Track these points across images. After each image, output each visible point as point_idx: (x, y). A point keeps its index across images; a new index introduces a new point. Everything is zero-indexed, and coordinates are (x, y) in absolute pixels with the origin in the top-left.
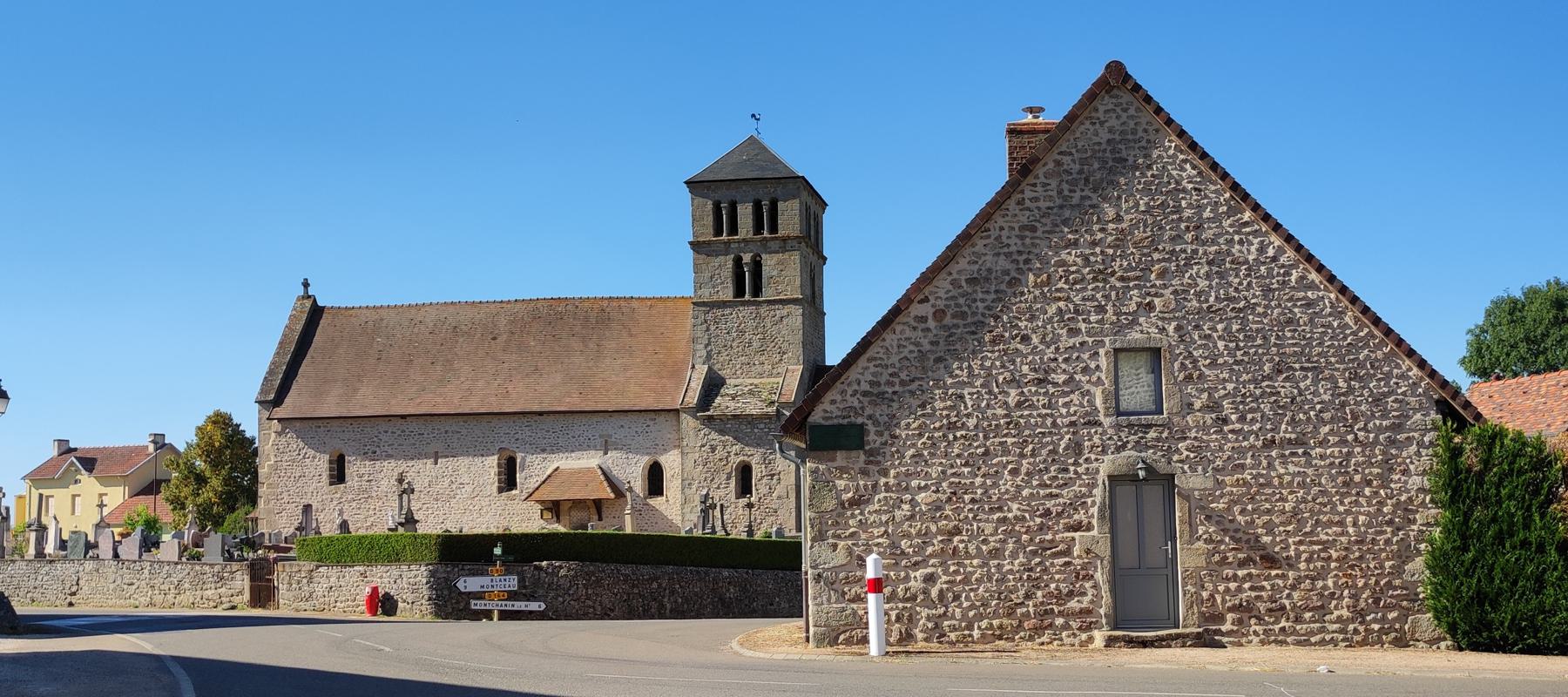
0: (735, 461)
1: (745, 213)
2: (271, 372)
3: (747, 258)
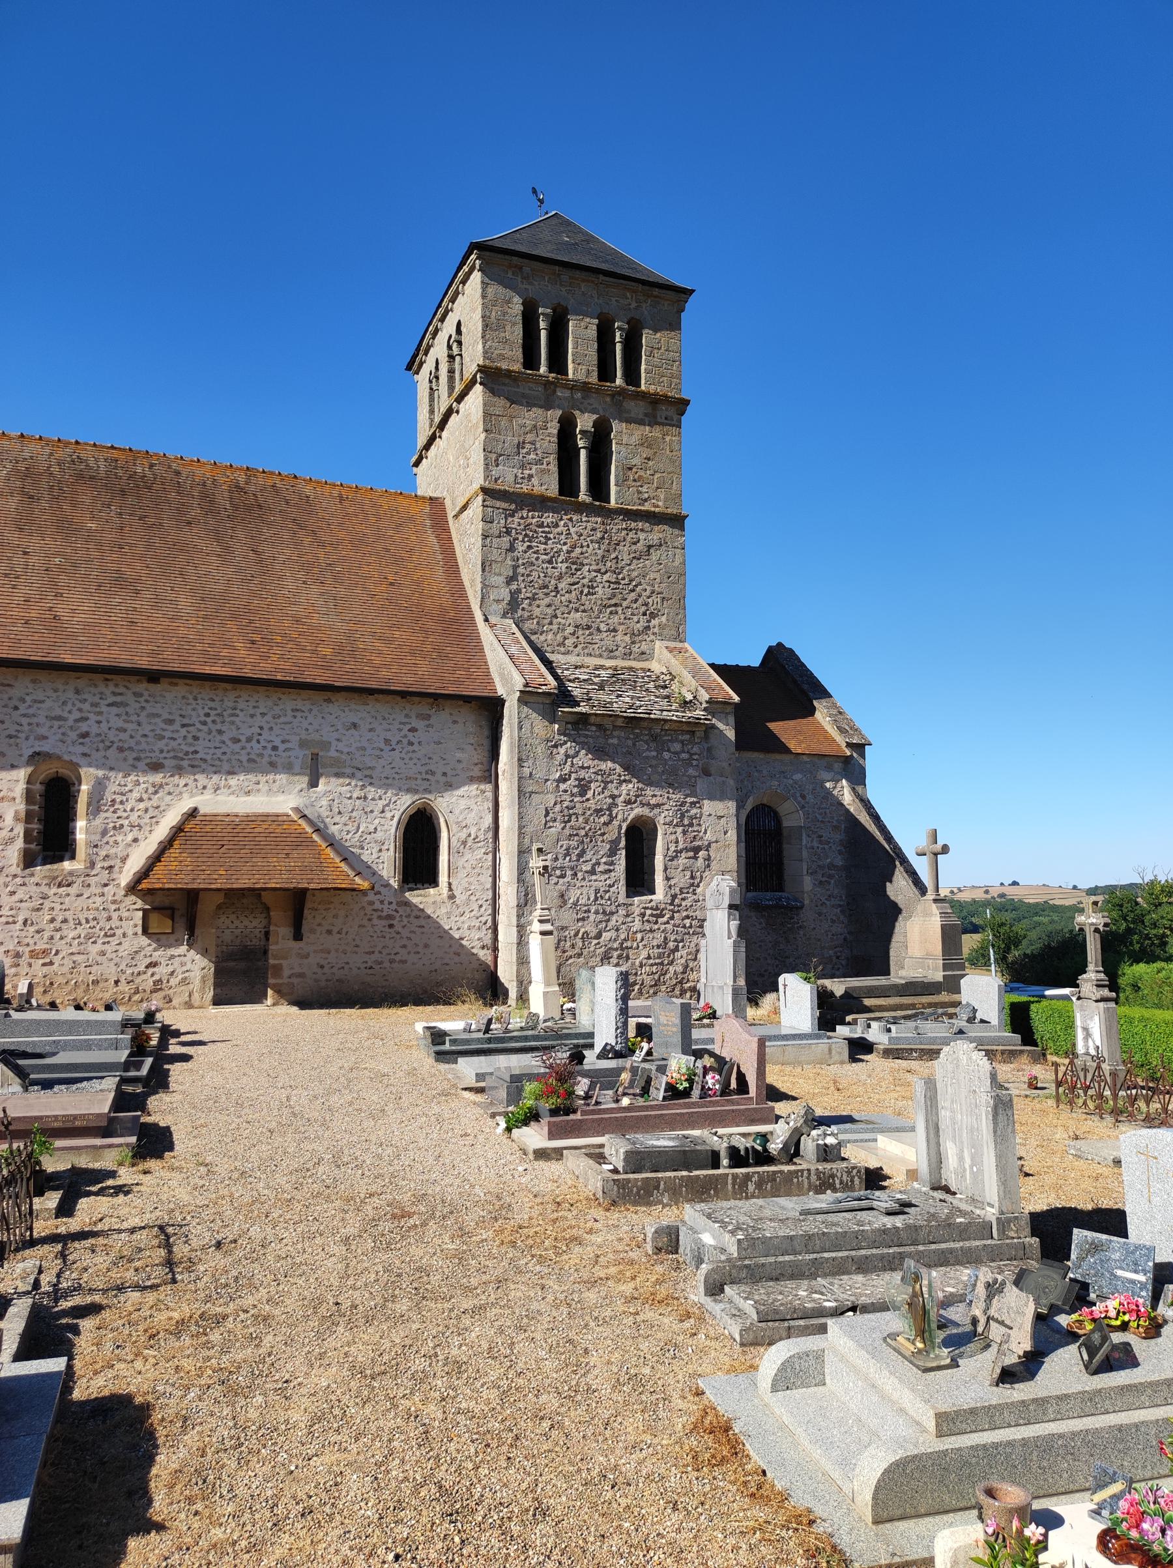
0: (627, 815)
1: (581, 335)
3: (585, 422)
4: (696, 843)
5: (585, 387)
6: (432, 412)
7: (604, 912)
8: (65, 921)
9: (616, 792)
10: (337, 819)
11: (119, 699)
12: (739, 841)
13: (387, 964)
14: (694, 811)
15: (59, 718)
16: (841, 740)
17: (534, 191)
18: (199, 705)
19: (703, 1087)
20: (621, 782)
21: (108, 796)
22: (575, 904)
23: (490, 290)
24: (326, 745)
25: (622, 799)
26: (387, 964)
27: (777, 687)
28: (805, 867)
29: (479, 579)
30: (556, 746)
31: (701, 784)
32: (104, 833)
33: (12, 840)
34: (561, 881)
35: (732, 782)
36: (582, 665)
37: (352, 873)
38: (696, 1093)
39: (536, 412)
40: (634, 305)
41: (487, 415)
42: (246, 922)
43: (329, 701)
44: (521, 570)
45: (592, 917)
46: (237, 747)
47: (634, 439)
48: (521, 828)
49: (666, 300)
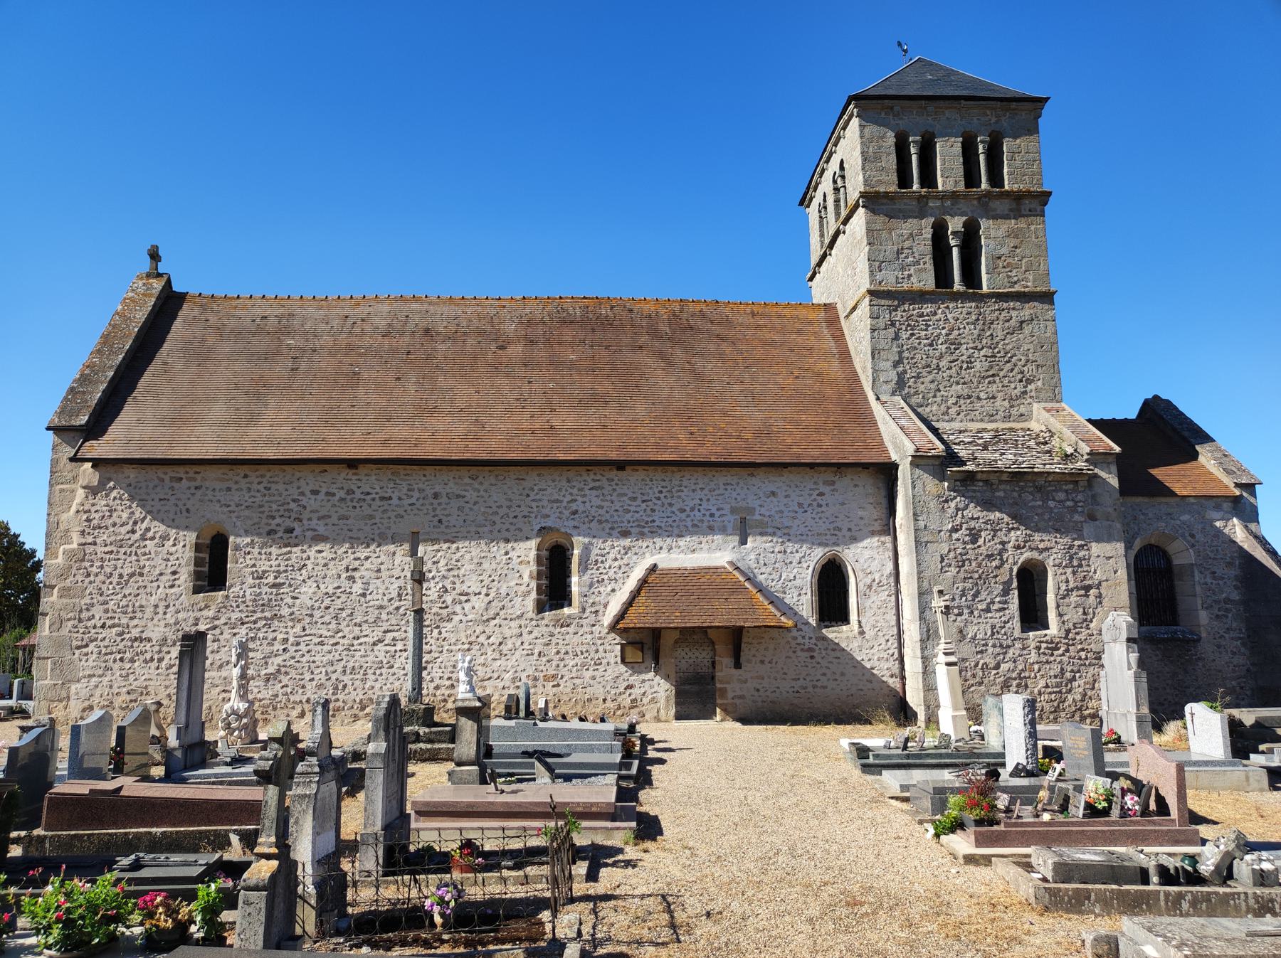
1: (948, 155)
2: (84, 379)
3: (955, 224)
4: (1086, 583)
5: (954, 196)
6: (822, 235)
7: (1001, 646)
8: (567, 653)
9: (1005, 539)
10: (763, 570)
11: (597, 484)
12: (1129, 580)
13: (810, 689)
14: (1082, 554)
15: (557, 501)
16: (1229, 482)
17: (900, 44)
18: (653, 485)
19: (1122, 808)
20: (1009, 530)
21: (593, 558)
22: (974, 638)
23: (866, 131)
24: (751, 511)
25: (1011, 544)
26: (810, 689)
27: (1158, 435)
28: (1199, 602)
29: (869, 365)
30: (947, 501)
31: (1088, 529)
32: (591, 586)
33: (528, 593)
34: (959, 618)
35: (1118, 526)
36: (967, 431)
37: (778, 614)
38: (1115, 812)
39: (912, 223)
40: (994, 120)
41: (870, 231)
42: (697, 654)
43: (752, 475)
44: (906, 354)
45: (990, 650)
46: (683, 516)
47: (1001, 233)
48: (919, 573)
49: (1024, 111)
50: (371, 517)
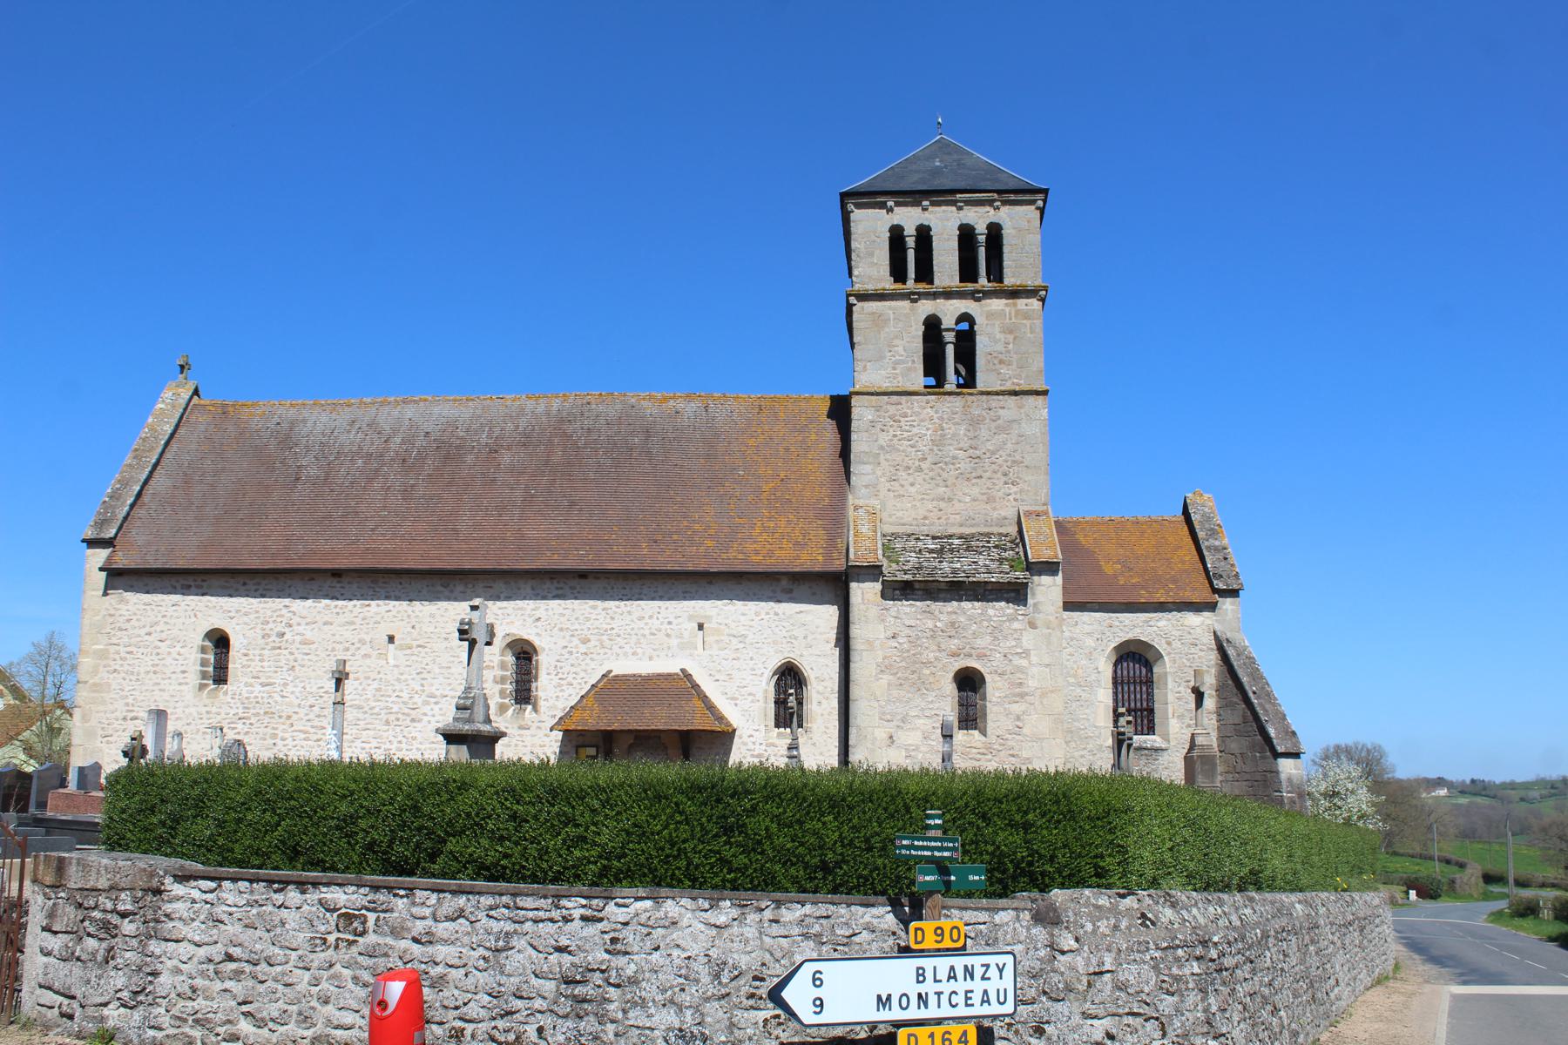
46: (641, 624)
50: (353, 623)
